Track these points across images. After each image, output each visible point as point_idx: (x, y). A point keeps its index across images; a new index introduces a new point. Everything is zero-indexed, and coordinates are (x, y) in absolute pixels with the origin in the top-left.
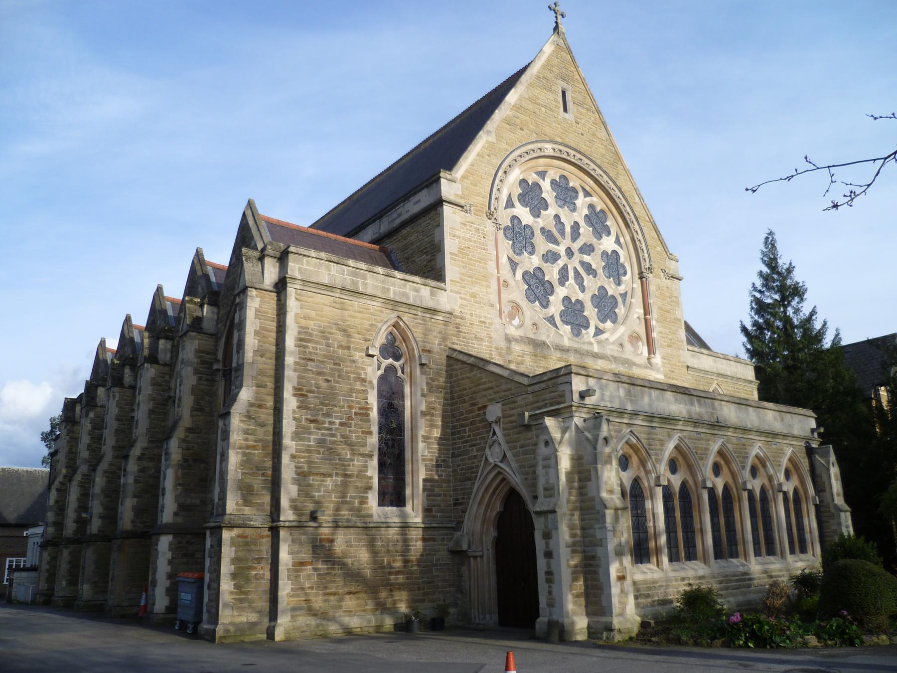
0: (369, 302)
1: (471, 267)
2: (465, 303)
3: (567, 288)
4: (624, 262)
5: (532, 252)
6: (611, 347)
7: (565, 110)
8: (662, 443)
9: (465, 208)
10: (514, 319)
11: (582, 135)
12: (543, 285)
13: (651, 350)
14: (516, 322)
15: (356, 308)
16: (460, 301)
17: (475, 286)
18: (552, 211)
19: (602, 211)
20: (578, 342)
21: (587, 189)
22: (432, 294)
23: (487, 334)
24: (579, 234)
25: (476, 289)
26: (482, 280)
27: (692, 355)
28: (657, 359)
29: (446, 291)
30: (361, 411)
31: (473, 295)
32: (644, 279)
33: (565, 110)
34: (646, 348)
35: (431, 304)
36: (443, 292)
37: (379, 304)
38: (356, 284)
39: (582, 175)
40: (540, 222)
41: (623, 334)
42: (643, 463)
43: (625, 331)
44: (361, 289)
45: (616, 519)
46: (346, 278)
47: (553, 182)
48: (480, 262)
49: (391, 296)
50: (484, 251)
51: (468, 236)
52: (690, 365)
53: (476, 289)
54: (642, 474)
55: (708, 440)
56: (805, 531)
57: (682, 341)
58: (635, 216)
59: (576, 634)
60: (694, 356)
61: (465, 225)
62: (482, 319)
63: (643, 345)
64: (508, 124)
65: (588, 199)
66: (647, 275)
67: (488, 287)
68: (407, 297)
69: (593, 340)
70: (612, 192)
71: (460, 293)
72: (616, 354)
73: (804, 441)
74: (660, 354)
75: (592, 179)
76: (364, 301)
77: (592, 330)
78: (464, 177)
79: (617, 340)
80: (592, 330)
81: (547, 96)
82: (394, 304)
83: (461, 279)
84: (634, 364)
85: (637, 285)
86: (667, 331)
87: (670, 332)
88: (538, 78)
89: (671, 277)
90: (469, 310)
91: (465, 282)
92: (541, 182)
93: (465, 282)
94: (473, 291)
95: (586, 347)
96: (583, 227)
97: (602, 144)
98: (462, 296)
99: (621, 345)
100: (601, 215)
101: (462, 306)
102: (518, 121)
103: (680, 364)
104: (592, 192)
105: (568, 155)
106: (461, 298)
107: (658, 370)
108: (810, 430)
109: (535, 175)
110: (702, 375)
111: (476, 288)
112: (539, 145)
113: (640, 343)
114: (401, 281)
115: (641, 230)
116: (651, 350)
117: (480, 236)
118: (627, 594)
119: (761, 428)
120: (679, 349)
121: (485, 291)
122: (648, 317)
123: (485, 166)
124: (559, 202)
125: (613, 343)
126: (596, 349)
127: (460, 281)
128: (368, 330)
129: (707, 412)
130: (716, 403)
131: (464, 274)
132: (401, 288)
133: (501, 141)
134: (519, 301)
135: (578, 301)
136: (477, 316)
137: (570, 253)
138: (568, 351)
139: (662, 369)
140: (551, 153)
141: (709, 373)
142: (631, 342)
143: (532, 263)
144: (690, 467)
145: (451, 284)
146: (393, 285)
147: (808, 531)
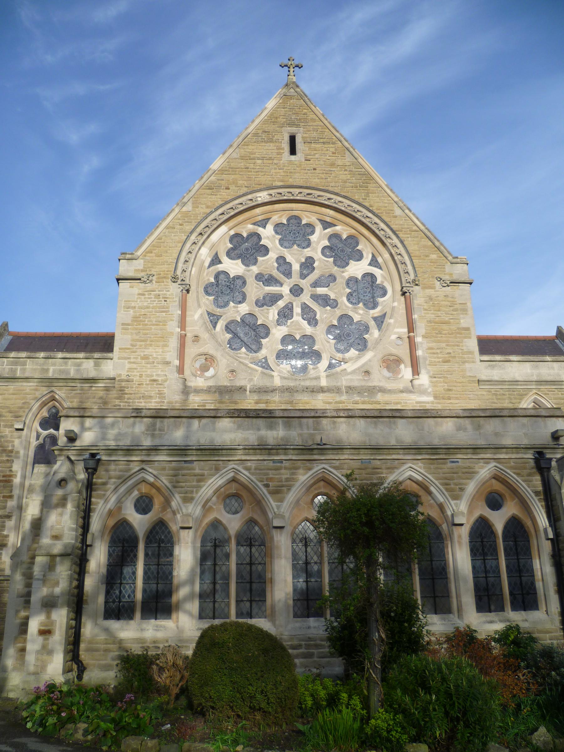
0: (25, 384)
1: (144, 331)
2: (134, 366)
3: (288, 327)
4: (382, 282)
5: (243, 299)
6: (349, 377)
7: (293, 151)
8: (201, 478)
9: (142, 279)
10: (208, 370)
11: (315, 169)
12: (254, 330)
13: (416, 371)
14: (211, 372)
15: (11, 392)
16: (128, 366)
17: (148, 349)
18: (273, 255)
19: (350, 237)
20: (296, 380)
21: (328, 220)
22: (97, 365)
23: (159, 391)
24: (314, 269)
25: (149, 351)
26: (158, 341)
27: (489, 366)
28: (424, 379)
29: (112, 359)
30: (4, 479)
31: (145, 358)
32: (408, 294)
33: (293, 151)
34: (409, 370)
35: (92, 374)
36: (109, 361)
37: (35, 384)
38: (15, 371)
39: (317, 208)
40: (255, 269)
41: (370, 360)
42: (167, 503)
43: (375, 356)
44: (18, 374)
45: (51, 567)
46: (4, 369)
47: (278, 227)
48: (157, 325)
49: (50, 374)
50: (164, 314)
51: (145, 304)
52: (484, 378)
53: (149, 351)
54: (167, 517)
55: (297, 468)
56: (536, 578)
57: (471, 353)
58: (391, 229)
59: (8, 691)
60: (493, 367)
61: (143, 295)
62: (155, 378)
63: (406, 367)
64: (209, 189)
65: (329, 231)
66: (411, 289)
67: (166, 346)
68: (68, 372)
69: (323, 374)
70: (357, 215)
71: (129, 358)
72: (356, 384)
73: (532, 451)
74: (428, 373)
75: (331, 209)
76: (20, 384)
77: (324, 364)
78: (148, 252)
79: (359, 369)
80: (324, 364)
81: (266, 148)
82: (49, 382)
83: (132, 345)
84: (383, 390)
85: (400, 304)
86: (444, 345)
87: (447, 345)
88: (256, 135)
89: (451, 283)
90: (138, 372)
91: (137, 347)
92: (260, 230)
93: (137, 347)
94: (145, 353)
95: (314, 383)
96: (320, 260)
97: (345, 170)
98: (132, 360)
99: (367, 372)
100: (350, 241)
101: (130, 369)
102: (223, 182)
103: (464, 380)
104: (335, 222)
105: (293, 195)
106: (130, 363)
107: (423, 392)
108: (550, 434)
109: (250, 227)
110: (507, 387)
111: (150, 350)
112: (250, 197)
113: (402, 366)
114: (62, 360)
115: (402, 242)
116: (416, 371)
117: (161, 301)
118: (50, 652)
119: (422, 443)
120: (464, 362)
121: (161, 350)
122: (411, 334)
123: (175, 236)
124: (286, 244)
125: (353, 372)
126: (324, 382)
127: (131, 347)
128: (21, 408)
129: (300, 435)
130: (324, 421)
131: (133, 340)
132: (61, 366)
133: (198, 207)
134: (212, 352)
135: (304, 336)
136: (147, 376)
137: (296, 291)
138: (273, 391)
139: (429, 390)
140: (267, 199)
141: (520, 383)
142: (388, 368)
143: (238, 311)
144: (259, 503)
145: (119, 352)
146: (54, 365)
147: (540, 577)
